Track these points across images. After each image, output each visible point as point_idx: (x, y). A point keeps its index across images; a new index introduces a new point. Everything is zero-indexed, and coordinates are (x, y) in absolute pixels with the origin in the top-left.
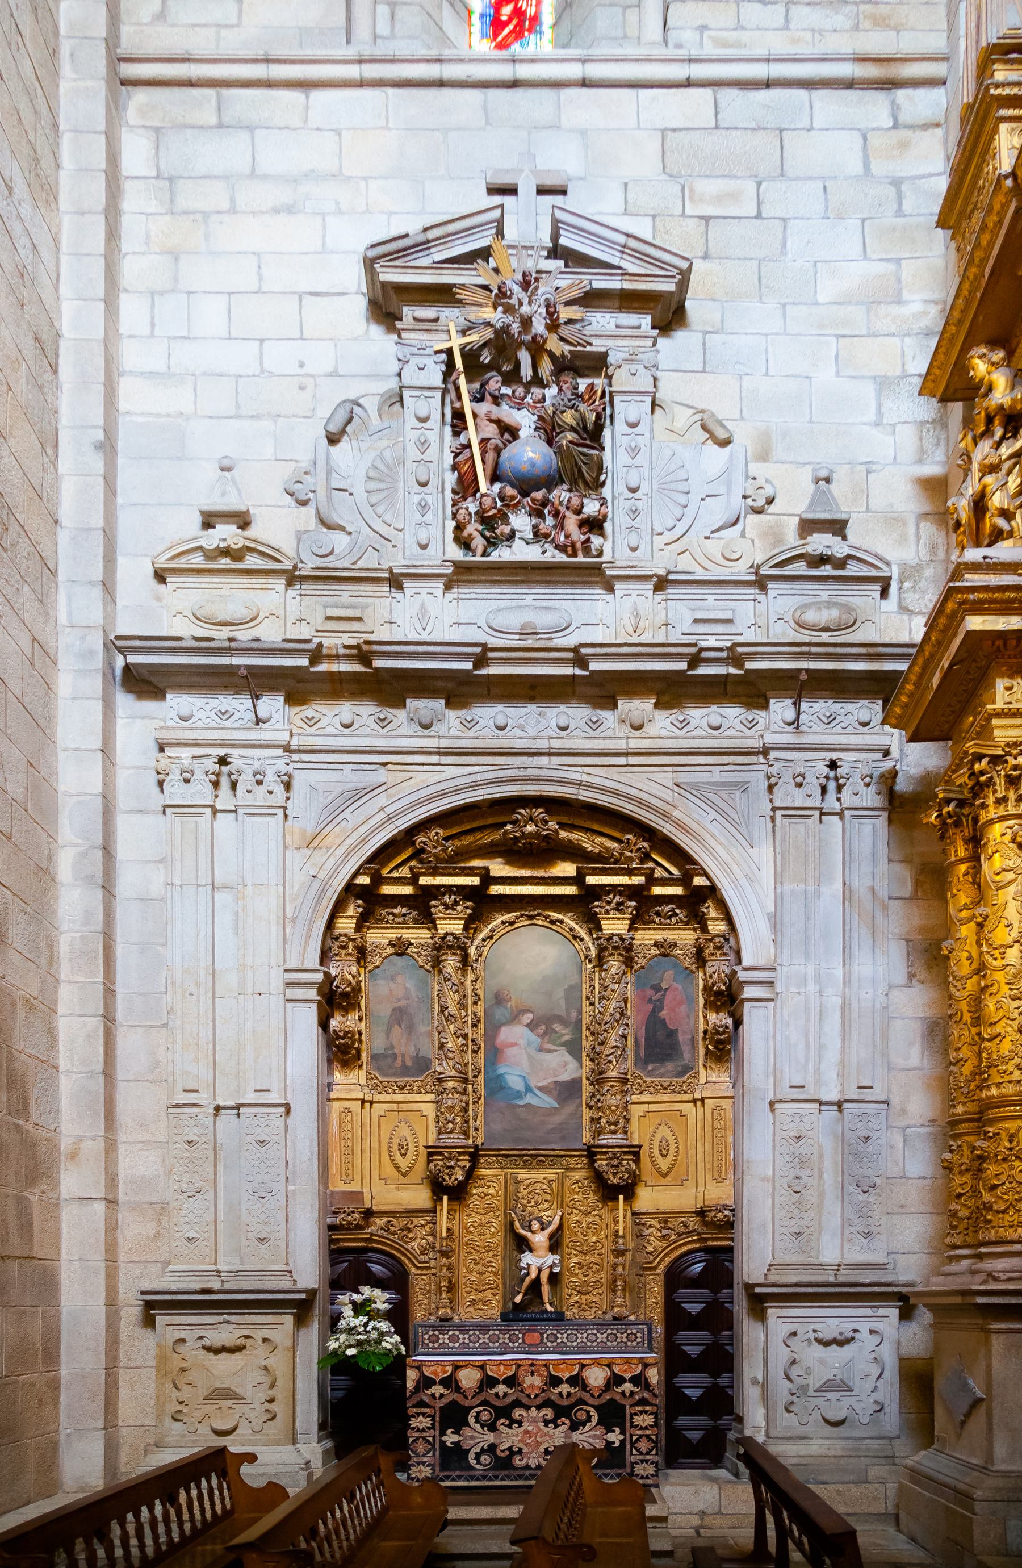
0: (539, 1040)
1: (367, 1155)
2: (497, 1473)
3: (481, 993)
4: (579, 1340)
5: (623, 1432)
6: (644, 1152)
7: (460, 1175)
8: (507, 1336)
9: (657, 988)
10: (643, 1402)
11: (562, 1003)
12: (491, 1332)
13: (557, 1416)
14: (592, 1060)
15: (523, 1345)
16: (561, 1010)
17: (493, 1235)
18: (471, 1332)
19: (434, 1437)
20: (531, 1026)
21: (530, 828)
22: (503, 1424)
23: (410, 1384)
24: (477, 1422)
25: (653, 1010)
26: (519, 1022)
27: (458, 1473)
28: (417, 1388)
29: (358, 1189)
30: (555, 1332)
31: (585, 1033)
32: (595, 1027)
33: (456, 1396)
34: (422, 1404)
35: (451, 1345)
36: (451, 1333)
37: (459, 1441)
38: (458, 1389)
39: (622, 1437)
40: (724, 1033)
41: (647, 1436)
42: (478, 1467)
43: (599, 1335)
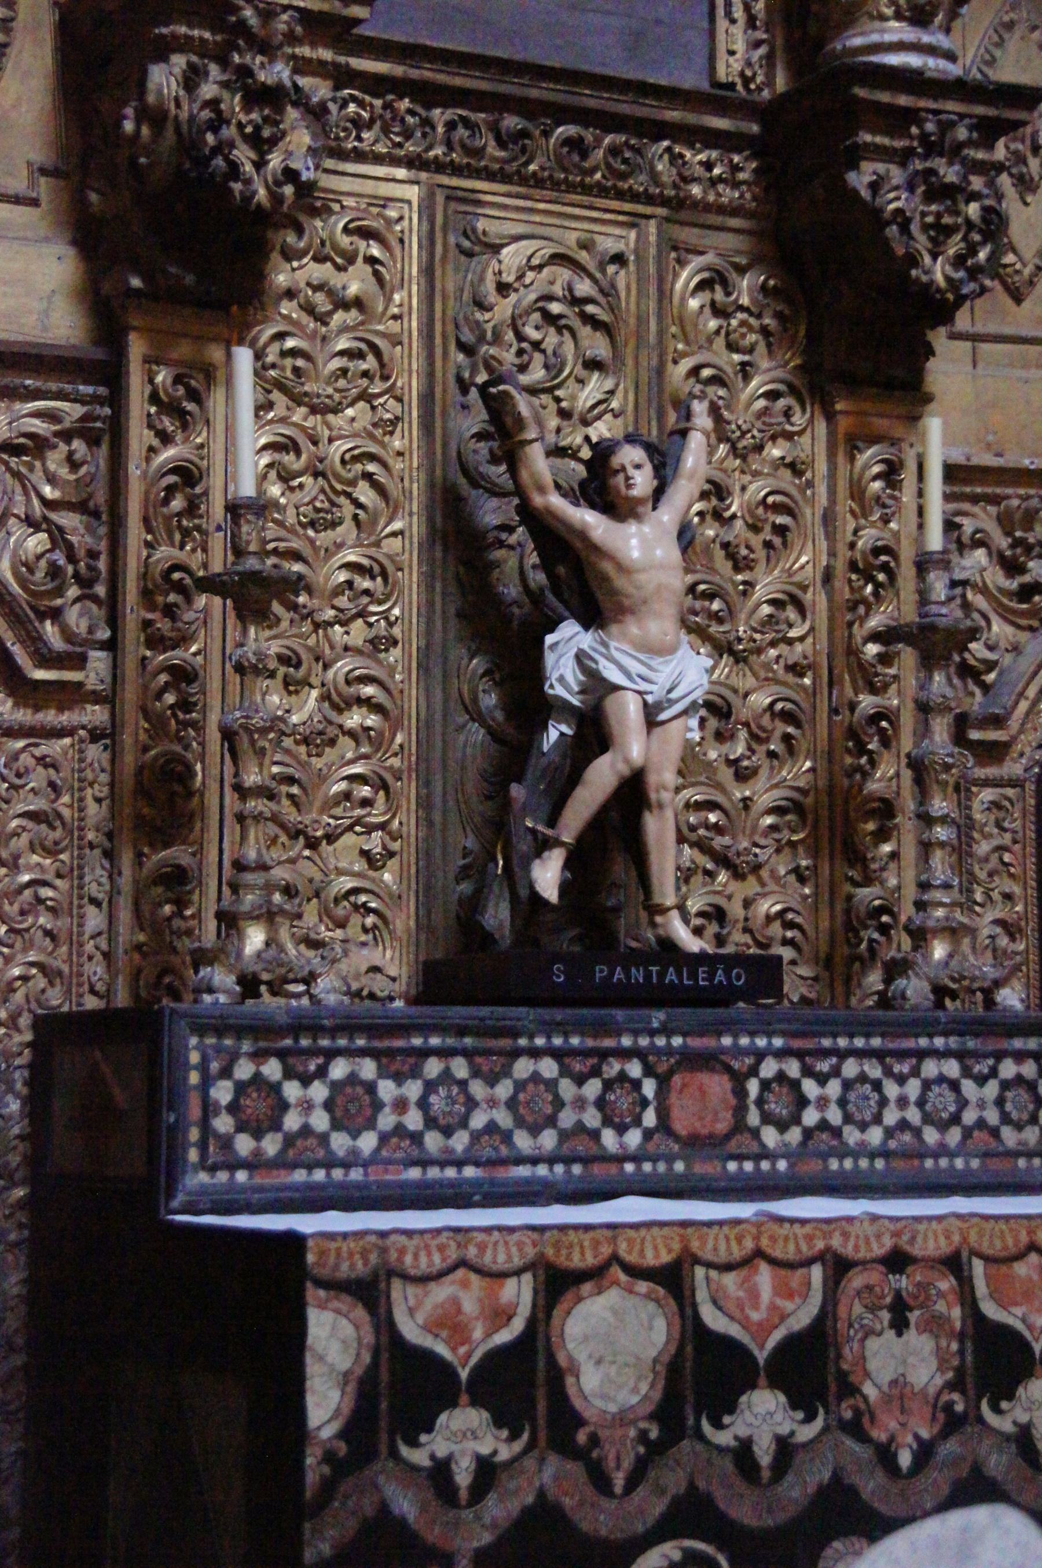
4: (891, 1117)
8: (593, 1088)
12: (523, 1067)
15: (662, 1144)
18: (433, 1067)
30: (793, 1068)
35: (340, 1142)
36: (339, 1070)
43: (968, 1087)
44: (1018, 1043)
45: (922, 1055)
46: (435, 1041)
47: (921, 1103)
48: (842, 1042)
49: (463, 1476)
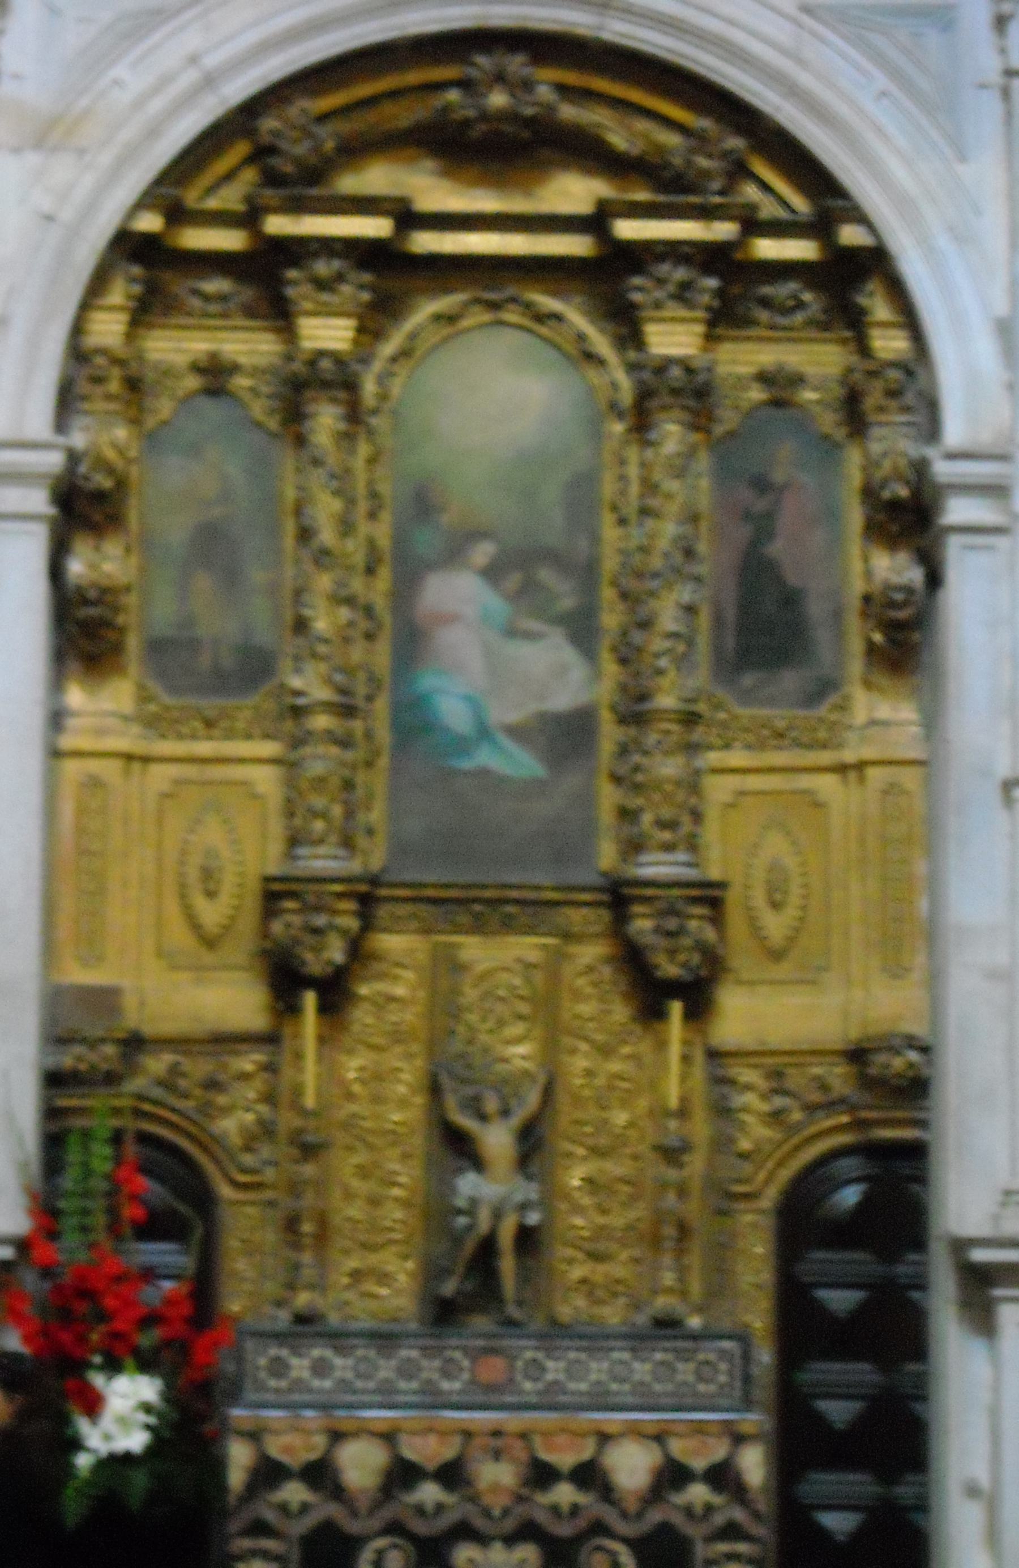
3: (385, 488)
6: (732, 898)
9: (761, 484)
14: (623, 661)
17: (403, 1103)
20: (492, 573)
21: (498, 99)
31: (608, 594)
32: (632, 584)
40: (904, 604)
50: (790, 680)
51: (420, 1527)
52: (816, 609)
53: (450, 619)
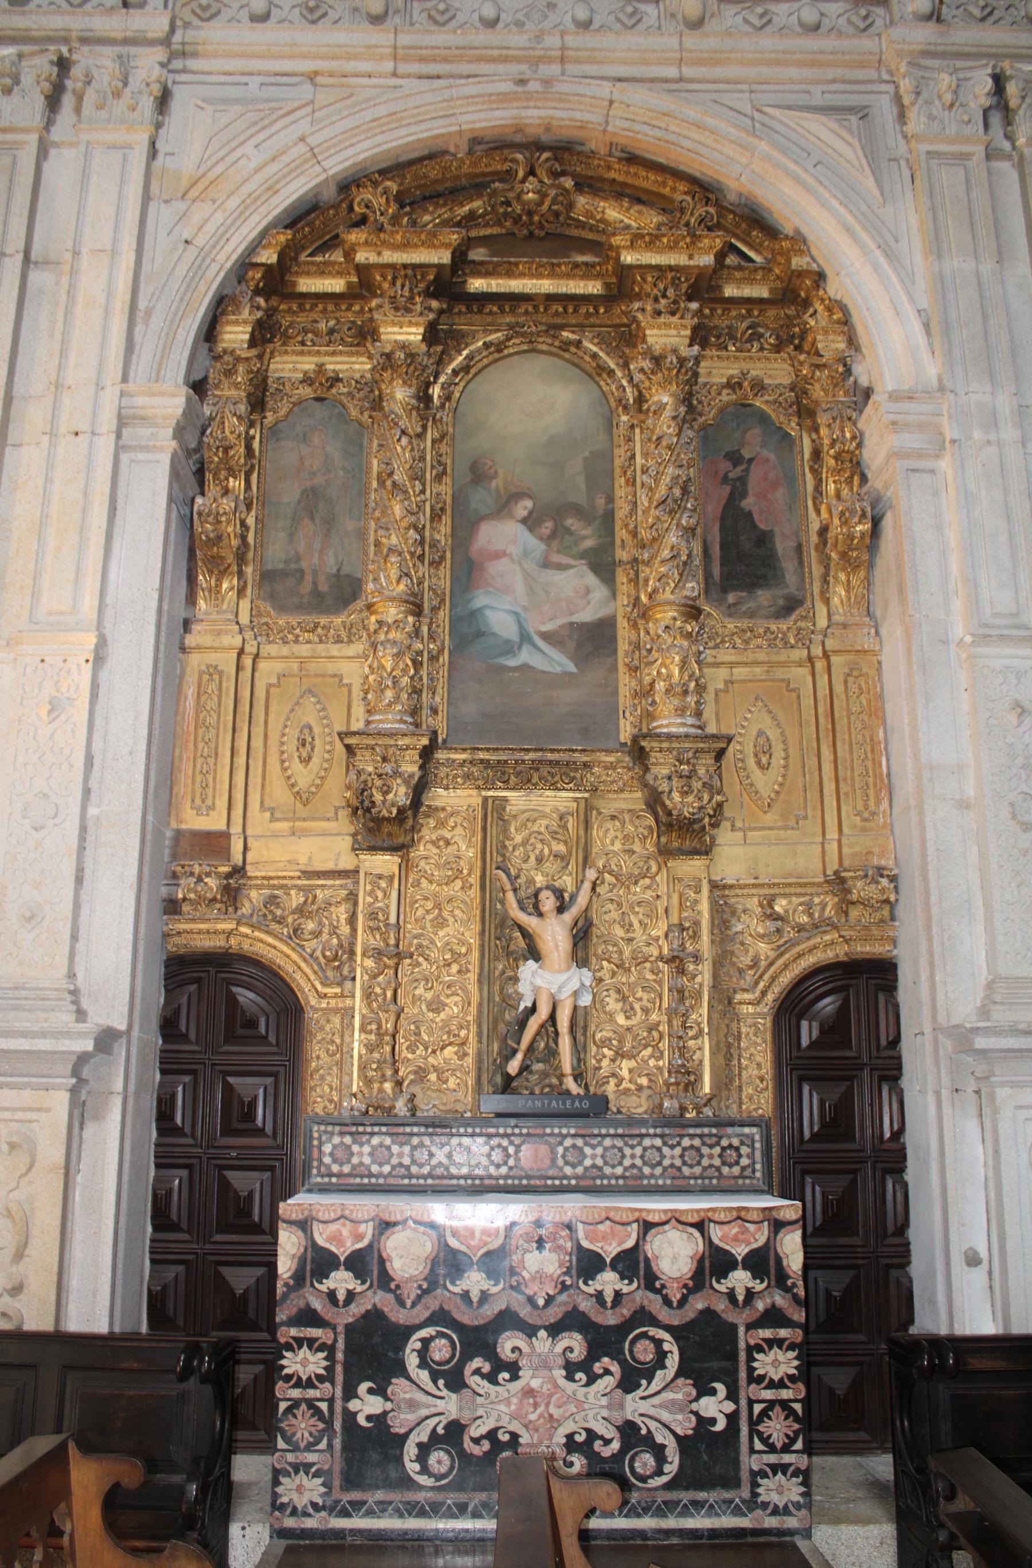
0: (543, 547)
1: (241, 760)
2: (462, 1497)
4: (627, 1162)
5: (732, 1395)
7: (401, 795)
9: (735, 458)
10: (773, 1317)
11: (581, 481)
13: (593, 1356)
16: (578, 494)
19: (331, 1401)
20: (530, 522)
22: (477, 1372)
23: (285, 1267)
24: (423, 1364)
25: (732, 494)
26: (511, 515)
27: (380, 1495)
28: (299, 1278)
29: (221, 826)
33: (381, 1299)
34: (308, 1317)
37: (385, 1413)
38: (385, 1280)
39: (729, 1407)
41: (784, 1404)
42: (423, 1480)
44: (691, 1131)
45: (642, 1136)
46: (415, 1129)
47: (642, 1157)
48: (604, 1131)
49: (341, 1296)
50: (764, 597)
51: (466, 1317)
52: (782, 546)
53: (499, 555)
